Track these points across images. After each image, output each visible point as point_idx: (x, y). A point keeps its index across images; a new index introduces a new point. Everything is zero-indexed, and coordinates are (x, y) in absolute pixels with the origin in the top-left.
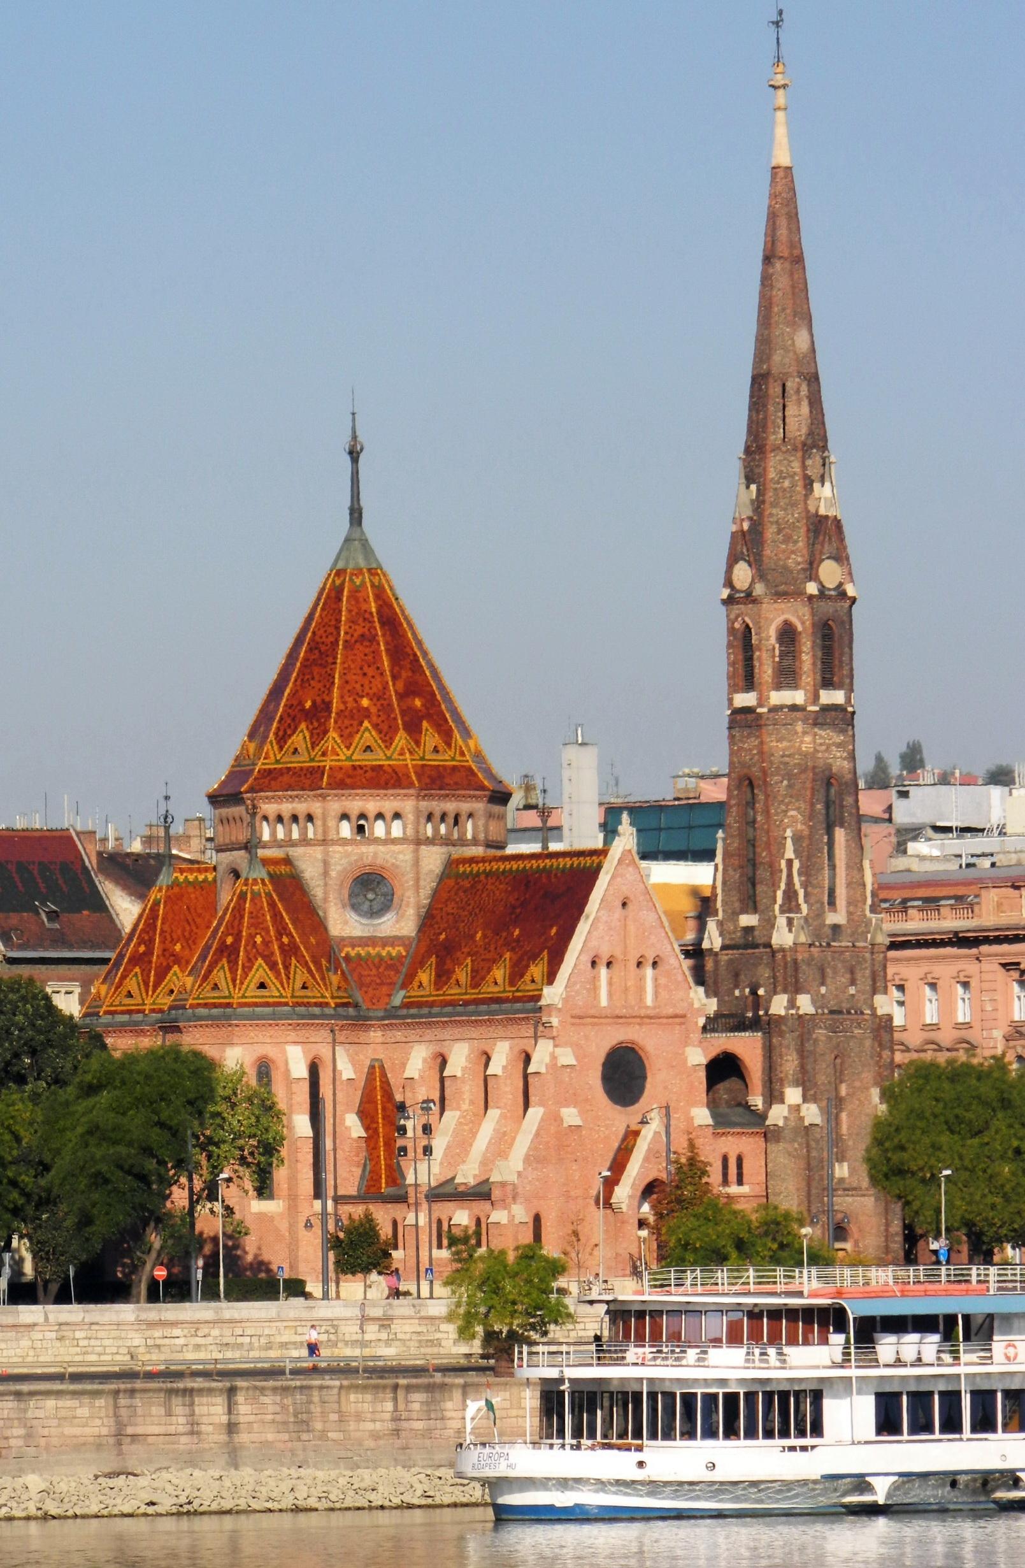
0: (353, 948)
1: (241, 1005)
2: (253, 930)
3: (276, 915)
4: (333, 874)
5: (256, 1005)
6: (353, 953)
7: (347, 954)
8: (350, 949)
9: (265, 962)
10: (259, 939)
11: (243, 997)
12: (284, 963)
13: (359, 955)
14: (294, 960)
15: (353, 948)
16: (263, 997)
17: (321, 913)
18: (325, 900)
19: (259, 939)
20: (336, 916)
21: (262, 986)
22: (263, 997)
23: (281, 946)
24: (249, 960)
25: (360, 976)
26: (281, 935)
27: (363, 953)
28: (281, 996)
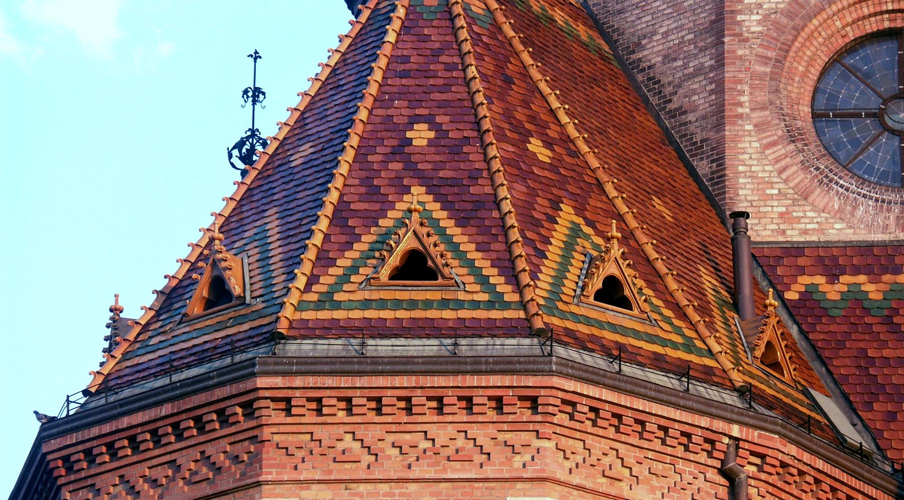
0: (833, 278)
1: (306, 331)
2: (400, 110)
3: (504, 78)
4: (751, 23)
5: (381, 330)
6: (833, 292)
7: (808, 294)
8: (820, 280)
9: (438, 198)
10: (421, 135)
11: (327, 301)
12: (525, 210)
13: (856, 299)
14: (567, 214)
15: (833, 278)
16: (413, 304)
17: (703, 168)
18: (719, 117)
19: (421, 135)
20: (765, 171)
21: (416, 267)
22: (413, 304)
23: (520, 166)
24: (372, 192)
25: (864, 361)
26: (526, 136)
27: (873, 290)
28: (497, 301)
